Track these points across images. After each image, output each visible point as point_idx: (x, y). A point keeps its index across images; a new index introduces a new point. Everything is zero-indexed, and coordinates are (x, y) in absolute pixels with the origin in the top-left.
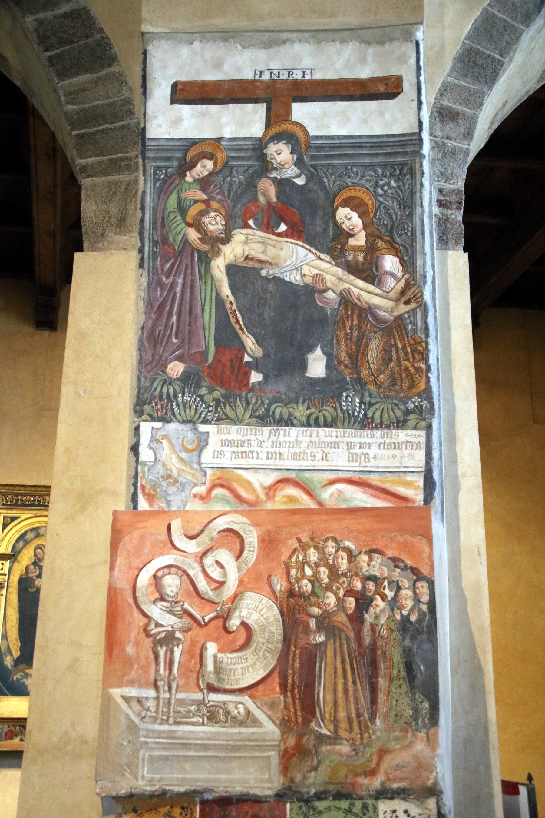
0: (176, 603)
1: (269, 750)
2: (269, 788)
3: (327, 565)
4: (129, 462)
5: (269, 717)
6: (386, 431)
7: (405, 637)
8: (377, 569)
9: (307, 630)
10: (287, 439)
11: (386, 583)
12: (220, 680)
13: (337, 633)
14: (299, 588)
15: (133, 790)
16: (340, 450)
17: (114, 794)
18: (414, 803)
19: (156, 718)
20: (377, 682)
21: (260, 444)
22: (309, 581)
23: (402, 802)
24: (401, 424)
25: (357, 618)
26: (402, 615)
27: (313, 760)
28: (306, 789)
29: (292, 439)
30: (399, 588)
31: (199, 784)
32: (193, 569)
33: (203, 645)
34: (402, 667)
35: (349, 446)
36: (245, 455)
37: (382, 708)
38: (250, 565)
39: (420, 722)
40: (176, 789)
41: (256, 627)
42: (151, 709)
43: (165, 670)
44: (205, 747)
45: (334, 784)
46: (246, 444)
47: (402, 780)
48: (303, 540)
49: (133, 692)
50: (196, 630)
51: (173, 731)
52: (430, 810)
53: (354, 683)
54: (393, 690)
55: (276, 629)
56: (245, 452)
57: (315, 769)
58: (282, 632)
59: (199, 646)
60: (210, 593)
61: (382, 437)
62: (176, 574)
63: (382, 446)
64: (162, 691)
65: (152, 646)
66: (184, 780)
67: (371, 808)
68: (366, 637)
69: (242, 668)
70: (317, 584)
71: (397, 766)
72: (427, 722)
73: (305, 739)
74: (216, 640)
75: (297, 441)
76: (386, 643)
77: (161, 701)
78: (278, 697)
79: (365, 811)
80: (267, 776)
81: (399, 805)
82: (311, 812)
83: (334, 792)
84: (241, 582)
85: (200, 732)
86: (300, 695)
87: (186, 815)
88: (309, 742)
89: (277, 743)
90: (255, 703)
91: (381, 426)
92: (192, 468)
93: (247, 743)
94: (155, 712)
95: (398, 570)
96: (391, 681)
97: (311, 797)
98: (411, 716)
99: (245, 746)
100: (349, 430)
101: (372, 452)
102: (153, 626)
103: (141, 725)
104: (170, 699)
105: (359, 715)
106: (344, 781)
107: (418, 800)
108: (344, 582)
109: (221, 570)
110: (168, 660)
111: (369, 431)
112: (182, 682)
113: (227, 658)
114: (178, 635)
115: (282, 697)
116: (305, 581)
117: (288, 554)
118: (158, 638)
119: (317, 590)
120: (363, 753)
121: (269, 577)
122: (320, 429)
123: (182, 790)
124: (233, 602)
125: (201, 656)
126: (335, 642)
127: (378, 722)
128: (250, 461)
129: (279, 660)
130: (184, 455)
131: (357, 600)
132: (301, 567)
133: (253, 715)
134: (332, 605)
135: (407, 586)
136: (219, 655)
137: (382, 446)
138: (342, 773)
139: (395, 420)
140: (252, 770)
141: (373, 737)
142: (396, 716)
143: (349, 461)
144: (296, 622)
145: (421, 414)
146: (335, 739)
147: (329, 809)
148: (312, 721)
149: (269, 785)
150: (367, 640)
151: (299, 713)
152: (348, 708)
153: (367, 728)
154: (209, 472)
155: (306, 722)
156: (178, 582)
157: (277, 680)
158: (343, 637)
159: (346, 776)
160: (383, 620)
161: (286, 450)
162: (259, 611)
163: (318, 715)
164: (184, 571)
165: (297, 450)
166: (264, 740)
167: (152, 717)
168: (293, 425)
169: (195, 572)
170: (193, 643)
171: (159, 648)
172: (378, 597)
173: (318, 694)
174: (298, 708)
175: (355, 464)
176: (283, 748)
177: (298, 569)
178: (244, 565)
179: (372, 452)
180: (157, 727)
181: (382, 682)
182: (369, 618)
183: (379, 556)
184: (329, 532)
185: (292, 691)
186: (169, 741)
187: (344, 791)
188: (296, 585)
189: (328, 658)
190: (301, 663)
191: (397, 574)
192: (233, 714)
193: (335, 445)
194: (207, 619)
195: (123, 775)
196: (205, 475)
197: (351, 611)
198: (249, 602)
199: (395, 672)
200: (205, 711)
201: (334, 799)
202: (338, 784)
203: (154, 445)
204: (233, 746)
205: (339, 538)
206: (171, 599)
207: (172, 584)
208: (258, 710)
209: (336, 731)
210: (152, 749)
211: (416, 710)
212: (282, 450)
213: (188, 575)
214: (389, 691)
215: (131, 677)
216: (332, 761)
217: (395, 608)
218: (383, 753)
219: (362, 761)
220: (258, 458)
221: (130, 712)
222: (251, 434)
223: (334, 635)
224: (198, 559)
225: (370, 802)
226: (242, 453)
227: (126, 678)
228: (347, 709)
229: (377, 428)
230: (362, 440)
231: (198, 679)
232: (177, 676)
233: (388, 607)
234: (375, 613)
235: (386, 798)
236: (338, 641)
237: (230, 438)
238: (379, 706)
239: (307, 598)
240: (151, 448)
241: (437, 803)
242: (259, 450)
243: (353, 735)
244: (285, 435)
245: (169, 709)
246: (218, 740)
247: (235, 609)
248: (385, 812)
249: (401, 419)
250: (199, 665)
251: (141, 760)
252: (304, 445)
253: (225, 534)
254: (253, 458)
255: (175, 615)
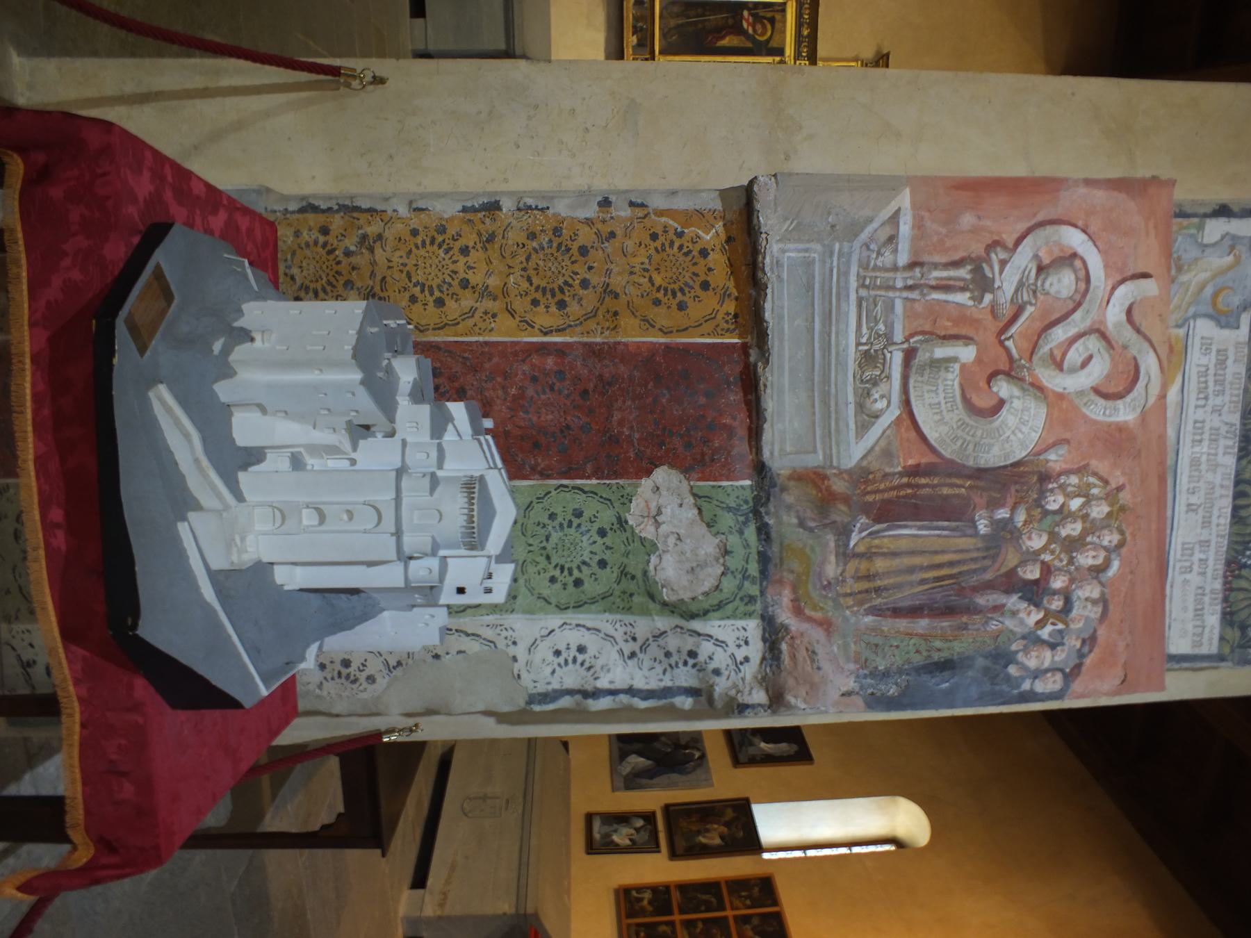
0: (1034, 292)
1: (824, 454)
2: (772, 453)
3: (1085, 533)
4: (1202, 204)
5: (872, 448)
6: (1220, 596)
7: (986, 657)
8: (1081, 612)
9: (993, 505)
10: (1221, 451)
11: (1060, 626)
12: (922, 369)
13: (991, 552)
14: (1052, 491)
15: (764, 236)
16: (1199, 530)
17: (758, 206)
18: (759, 672)
19: (866, 268)
20: (922, 617)
21: (1217, 410)
22: (1063, 506)
23: (760, 655)
24: (1228, 618)
25: (1011, 583)
26: (1017, 652)
27: (814, 520)
28: (773, 510)
29: (1221, 459)
30: (1053, 646)
31: (776, 344)
32: (1083, 319)
33: (971, 339)
34: (945, 655)
35: (1205, 544)
36: (1203, 389)
37: (888, 624)
38: (1084, 410)
39: (869, 681)
40: (768, 306)
41: (997, 424)
42: (881, 259)
43: (937, 279)
44: (826, 349)
45: (781, 552)
46: (1218, 388)
47: (793, 657)
48: (1121, 495)
49: (905, 228)
50: (994, 327)
51: (848, 296)
52: (750, 694)
53: (923, 582)
54: (912, 642)
55: (993, 456)
56: (1206, 388)
57: (802, 524)
58: (991, 464)
59: (971, 333)
60: (1046, 349)
61: (1212, 591)
62: (1076, 291)
63: (1200, 591)
64: (906, 274)
65: (973, 255)
66: (781, 317)
67: (750, 608)
68: (986, 597)
69: (939, 403)
70: (1057, 518)
71: (814, 652)
72: (869, 691)
73: (843, 508)
74: (979, 360)
75: (1217, 465)
76: (978, 630)
77: (891, 275)
78: (899, 464)
79: (746, 600)
80: (788, 449)
81: (756, 650)
82: (741, 519)
83: (769, 553)
84: (1061, 397)
85: (847, 339)
86: (903, 497)
87: (727, 322)
88: (840, 514)
89: (835, 464)
90: (889, 426)
91: (1228, 589)
92: (1190, 304)
93: (833, 416)
94: (875, 265)
95: (1078, 644)
96: (924, 637)
97: (761, 517)
98: (876, 668)
99: (830, 412)
100: (1226, 542)
101: (1194, 578)
102: (1003, 255)
103: (857, 244)
104: (893, 288)
105: (878, 590)
106: (785, 567)
107: (764, 679)
108: (1061, 561)
109: (1079, 364)
110: (951, 283)
111: (1221, 573)
112: (919, 307)
113: (953, 377)
114: (988, 298)
115: (900, 469)
116: (1061, 499)
117: (1101, 473)
118: (984, 265)
119: (1049, 517)
120: (826, 597)
121: (1067, 441)
122: (1230, 500)
123: (768, 315)
124: (1032, 384)
125: (956, 337)
126: (978, 549)
127: (869, 619)
128: (1193, 396)
129: (952, 462)
130: (1209, 291)
131: (1036, 582)
132: (1083, 492)
133: (873, 424)
134: (1029, 543)
135: (1057, 658)
136: (957, 366)
137: (1200, 591)
138: (796, 565)
139: (1234, 609)
140: (796, 424)
141: (848, 612)
142: (876, 645)
143: (1183, 544)
144: (1004, 487)
145: (1240, 646)
146: (844, 554)
147: (747, 546)
148: (868, 517)
149: (776, 453)
150: (981, 600)
151: (878, 497)
152: (888, 574)
153: (861, 603)
154: (1182, 332)
155: (866, 509)
156: (1065, 293)
157: (924, 461)
158: (988, 562)
159: (792, 572)
160: (1009, 623)
161: (1205, 450)
162: (1019, 429)
163: (877, 527)
164: (1079, 305)
165: (1203, 467)
166: (838, 444)
167: (868, 265)
168: (1239, 459)
169: (1079, 322)
170: (975, 322)
171: (969, 267)
172: (1041, 615)
173: (906, 527)
174: (886, 495)
175: (1179, 552)
176: (829, 472)
177: (1079, 487)
178: (1085, 400)
179: (1194, 578)
180: (854, 269)
181: (923, 624)
182: (1013, 601)
183: (1099, 615)
184: (1133, 535)
185: (909, 485)
186: (834, 291)
187: (771, 567)
188: (1055, 485)
189: (958, 541)
190: (947, 498)
191: (1073, 642)
192: (873, 391)
193: (1206, 523)
194: (1009, 344)
195: (786, 219)
196: (1178, 326)
197: (1021, 573)
198: (1032, 411)
199: (938, 644)
200: (877, 347)
201: (759, 552)
202: (781, 559)
203: (1227, 242)
204: (829, 392)
205: (1124, 550)
206: (1039, 283)
207: (1063, 283)
208: (880, 432)
209: (856, 556)
210: (823, 262)
211: (886, 675)
212: (1206, 443)
213: (1074, 310)
214: (911, 635)
215: (928, 223)
216: (812, 549)
217: (1024, 642)
218: (826, 625)
219: (815, 594)
220: (1197, 407)
221: (875, 225)
222: (1231, 395)
223: (987, 549)
224: (1096, 326)
225: (758, 607)
226: (1206, 382)
227: (927, 215)
228: (888, 573)
229: (1225, 583)
230: (1211, 563)
231: (923, 333)
232: (928, 298)
233: (1027, 630)
234: (1018, 611)
235: (764, 630)
236: (981, 554)
237: (1230, 362)
238: (890, 620)
239: (1038, 503)
240: (1223, 238)
241: (760, 705)
242: (1209, 409)
243: (850, 581)
244: (1227, 447)
245: (880, 288)
246: (836, 371)
247: (1023, 389)
248: (745, 629)
249: (1236, 618)
250: (943, 333)
251: (807, 246)
252: (1210, 476)
253: (1132, 367)
254: (1198, 399)
255: (1016, 291)
